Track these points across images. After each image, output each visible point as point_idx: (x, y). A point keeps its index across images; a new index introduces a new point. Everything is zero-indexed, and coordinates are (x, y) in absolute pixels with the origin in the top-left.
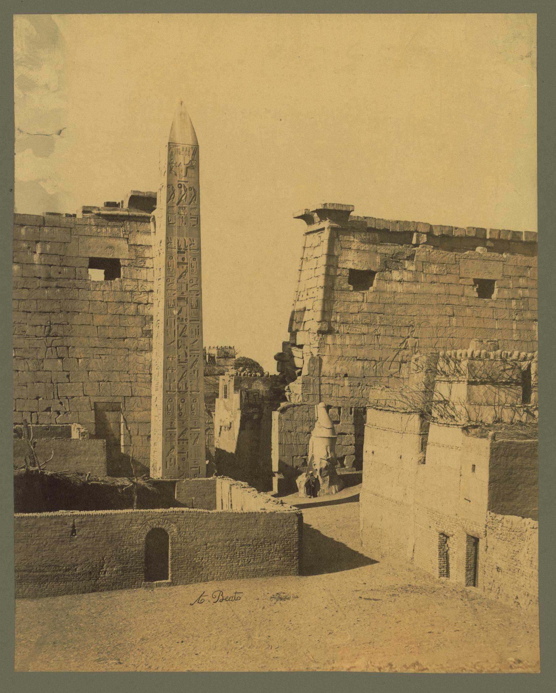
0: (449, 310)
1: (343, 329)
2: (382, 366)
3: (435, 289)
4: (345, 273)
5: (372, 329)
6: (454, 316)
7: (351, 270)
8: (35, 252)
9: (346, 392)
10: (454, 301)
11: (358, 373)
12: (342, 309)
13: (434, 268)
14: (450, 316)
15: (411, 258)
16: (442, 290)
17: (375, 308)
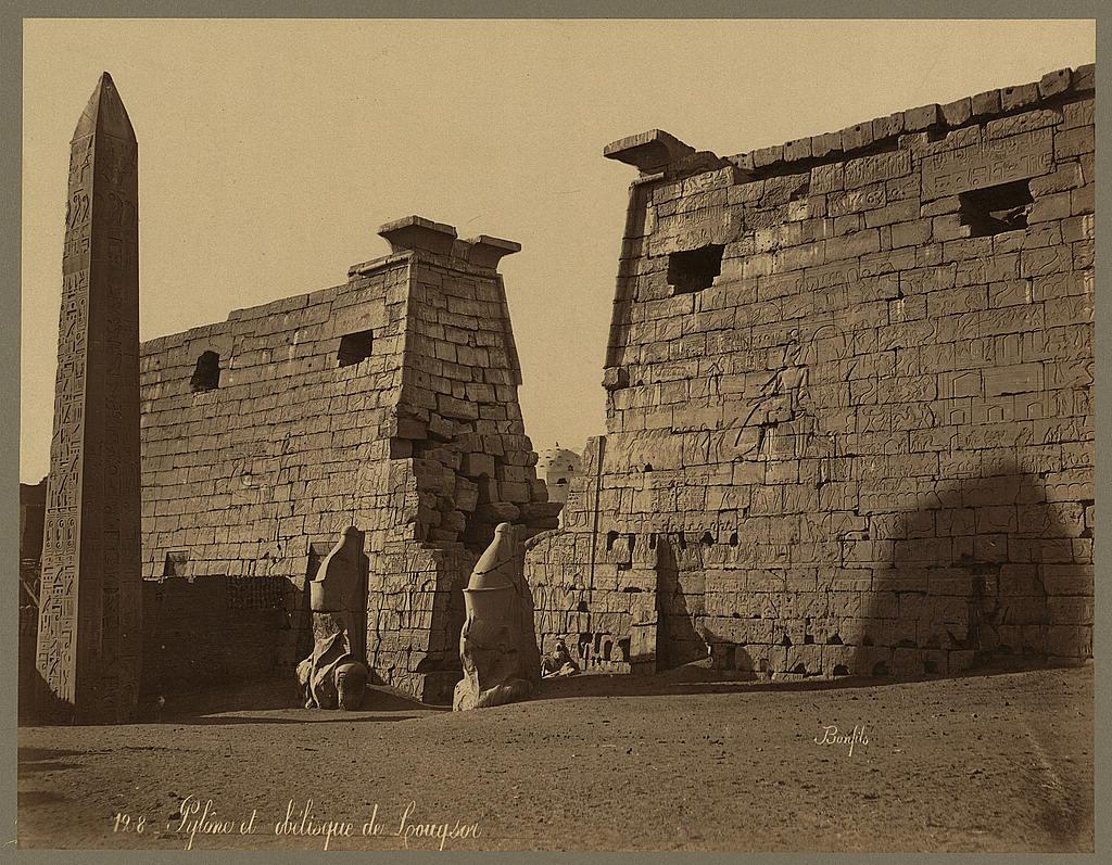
0: (888, 286)
1: (649, 376)
2: (721, 441)
3: (857, 245)
4: (663, 264)
5: (706, 365)
6: (901, 296)
7: (673, 255)
8: (292, 344)
9: (645, 502)
10: (900, 261)
11: (671, 462)
12: (652, 335)
13: (854, 200)
14: (888, 300)
15: (803, 190)
16: (872, 243)
17: (716, 319)
